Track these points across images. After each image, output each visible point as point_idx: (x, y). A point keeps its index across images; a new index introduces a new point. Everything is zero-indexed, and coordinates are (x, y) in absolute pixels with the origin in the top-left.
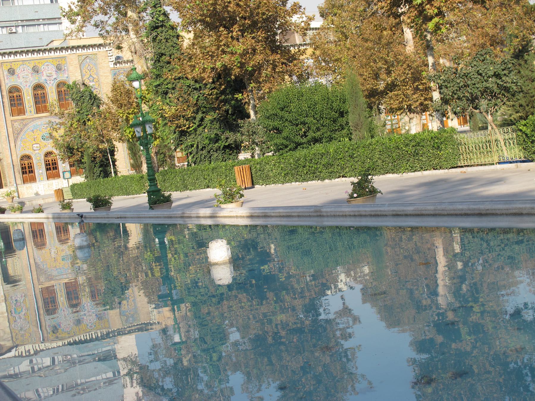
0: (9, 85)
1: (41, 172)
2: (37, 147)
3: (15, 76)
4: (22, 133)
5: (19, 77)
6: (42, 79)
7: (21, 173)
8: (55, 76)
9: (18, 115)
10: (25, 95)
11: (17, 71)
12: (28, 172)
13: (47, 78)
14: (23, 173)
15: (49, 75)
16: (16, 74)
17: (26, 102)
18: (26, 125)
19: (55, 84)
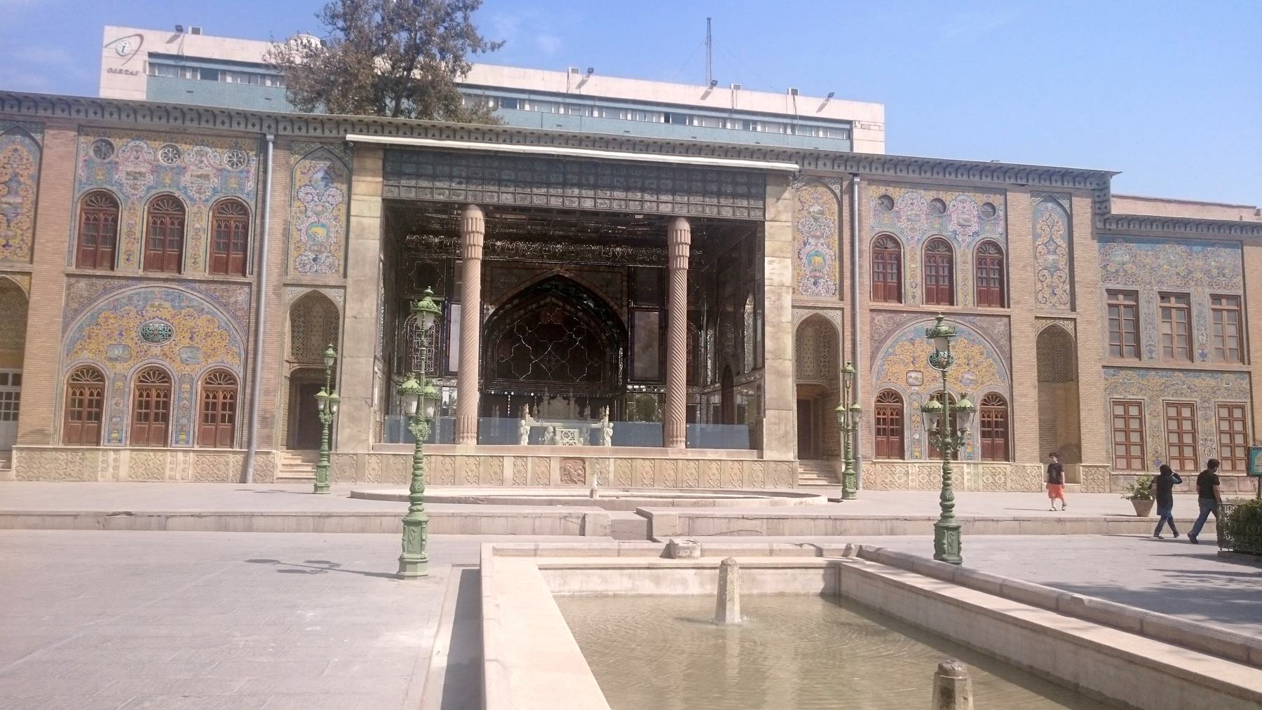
0: (878, 230)
1: (917, 436)
2: (916, 378)
4: (889, 342)
6: (949, 229)
7: (874, 432)
8: (975, 228)
9: (886, 300)
10: (908, 257)
11: (899, 204)
13: (959, 229)
14: (878, 432)
15: (963, 223)
16: (895, 209)
17: (908, 275)
18: (899, 325)
19: (974, 244)
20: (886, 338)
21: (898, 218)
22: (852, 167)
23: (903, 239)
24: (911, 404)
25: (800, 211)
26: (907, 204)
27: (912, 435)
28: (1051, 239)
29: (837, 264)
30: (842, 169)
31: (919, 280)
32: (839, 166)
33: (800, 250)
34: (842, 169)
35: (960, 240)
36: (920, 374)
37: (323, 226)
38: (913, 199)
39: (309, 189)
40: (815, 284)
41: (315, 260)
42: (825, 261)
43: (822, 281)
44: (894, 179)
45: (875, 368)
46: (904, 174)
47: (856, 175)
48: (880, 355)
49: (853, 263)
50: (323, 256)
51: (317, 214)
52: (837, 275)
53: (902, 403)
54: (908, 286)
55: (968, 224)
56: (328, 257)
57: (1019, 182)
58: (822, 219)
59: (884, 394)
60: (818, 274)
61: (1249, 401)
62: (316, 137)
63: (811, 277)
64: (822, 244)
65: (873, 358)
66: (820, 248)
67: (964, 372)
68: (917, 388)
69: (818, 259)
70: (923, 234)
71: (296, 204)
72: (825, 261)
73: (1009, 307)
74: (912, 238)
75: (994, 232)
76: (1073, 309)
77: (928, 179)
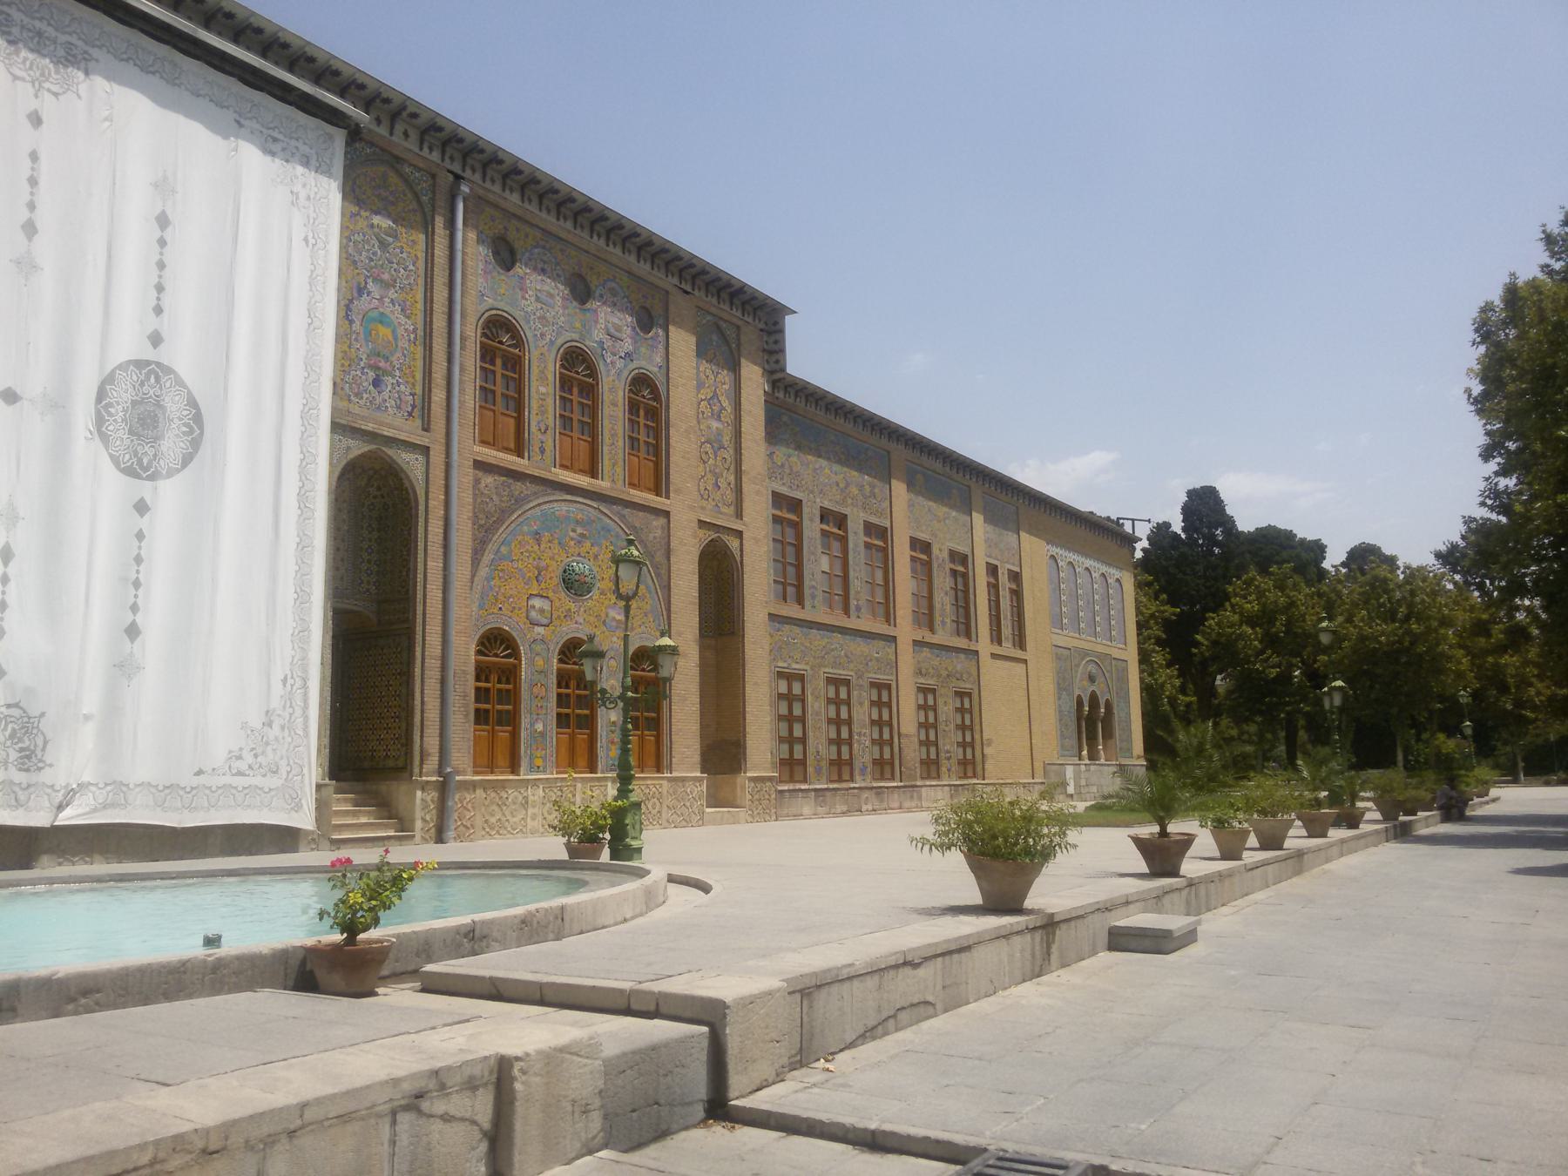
0: (490, 302)
2: (542, 611)
5: (523, 289)
7: (472, 716)
8: (627, 346)
10: (535, 371)
13: (608, 343)
15: (612, 331)
20: (500, 521)
21: (521, 289)
23: (529, 332)
24: (531, 661)
27: (532, 725)
28: (715, 395)
29: (419, 351)
31: (551, 422)
33: (351, 301)
35: (608, 361)
36: (547, 601)
38: (545, 262)
40: (376, 383)
42: (396, 339)
43: (389, 380)
44: (519, 212)
48: (488, 557)
49: (450, 360)
52: (419, 376)
54: (534, 429)
55: (617, 334)
57: (683, 286)
60: (382, 364)
61: (894, 678)
63: (370, 367)
64: (392, 301)
66: (388, 309)
67: (608, 607)
68: (540, 630)
69: (384, 332)
70: (559, 334)
72: (396, 339)
73: (668, 497)
74: (542, 335)
75: (650, 364)
76: (739, 514)
77: (569, 232)
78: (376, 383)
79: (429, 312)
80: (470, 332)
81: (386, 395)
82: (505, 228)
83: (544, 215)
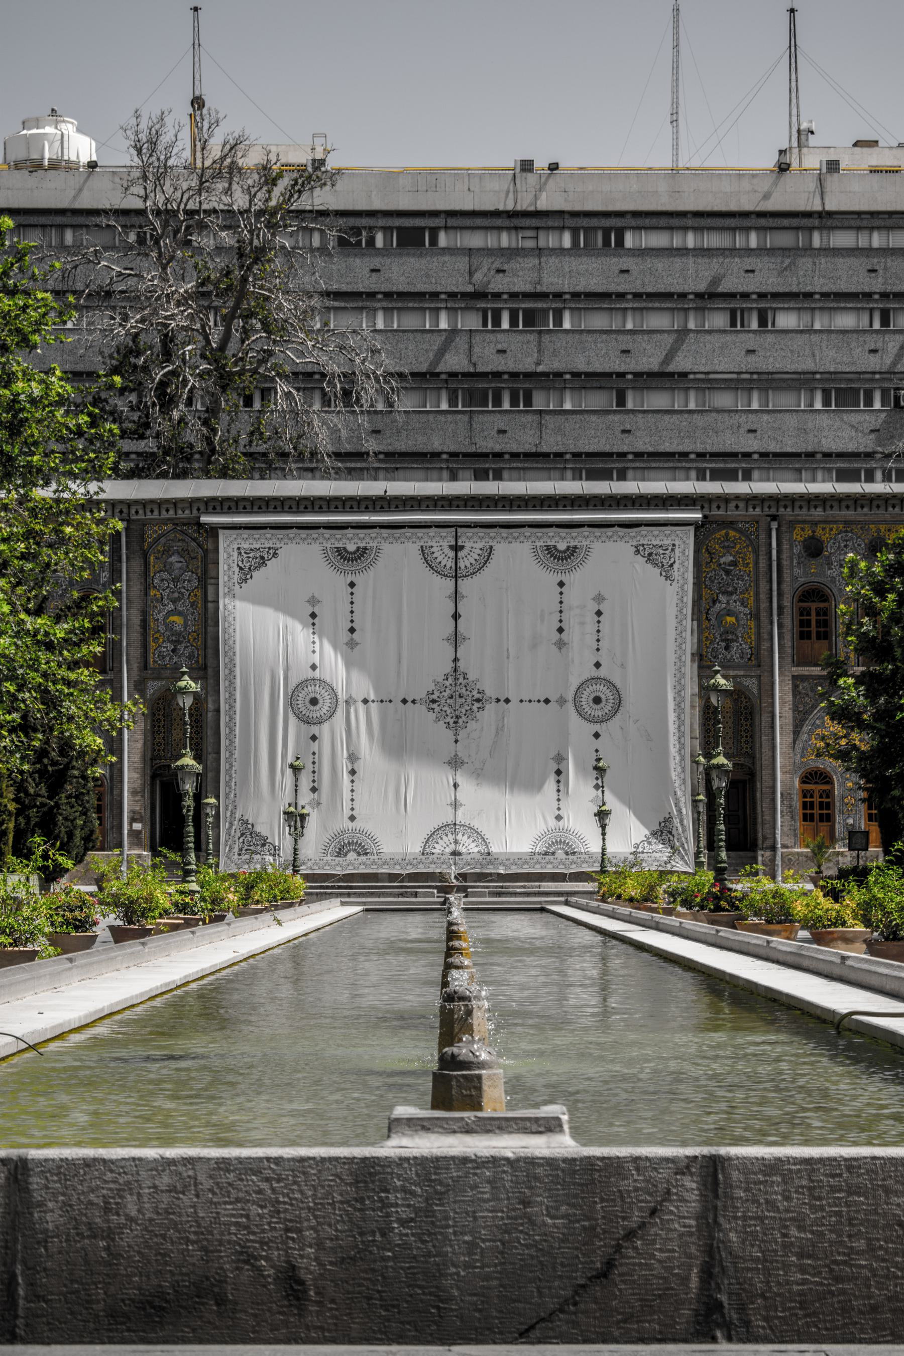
0: (802, 580)
3: (820, 560)
5: (829, 564)
11: (829, 549)
12: (816, 817)
22: (770, 507)
24: (842, 784)
25: (707, 563)
26: (839, 547)
30: (758, 510)
32: (754, 508)
34: (758, 510)
37: (180, 614)
39: (165, 575)
40: (727, 648)
41: (174, 651)
45: (799, 745)
46: (835, 512)
47: (774, 518)
48: (806, 729)
50: (181, 647)
51: (174, 601)
53: (832, 783)
56: (186, 647)
58: (735, 571)
59: (810, 774)
60: (730, 637)
62: (168, 519)
63: (722, 641)
65: (796, 732)
69: (729, 619)
71: (153, 592)
72: (737, 620)
77: (865, 515)
78: (727, 648)
79: (757, 600)
80: (787, 603)
81: (733, 652)
82: (814, 532)
83: (844, 512)
